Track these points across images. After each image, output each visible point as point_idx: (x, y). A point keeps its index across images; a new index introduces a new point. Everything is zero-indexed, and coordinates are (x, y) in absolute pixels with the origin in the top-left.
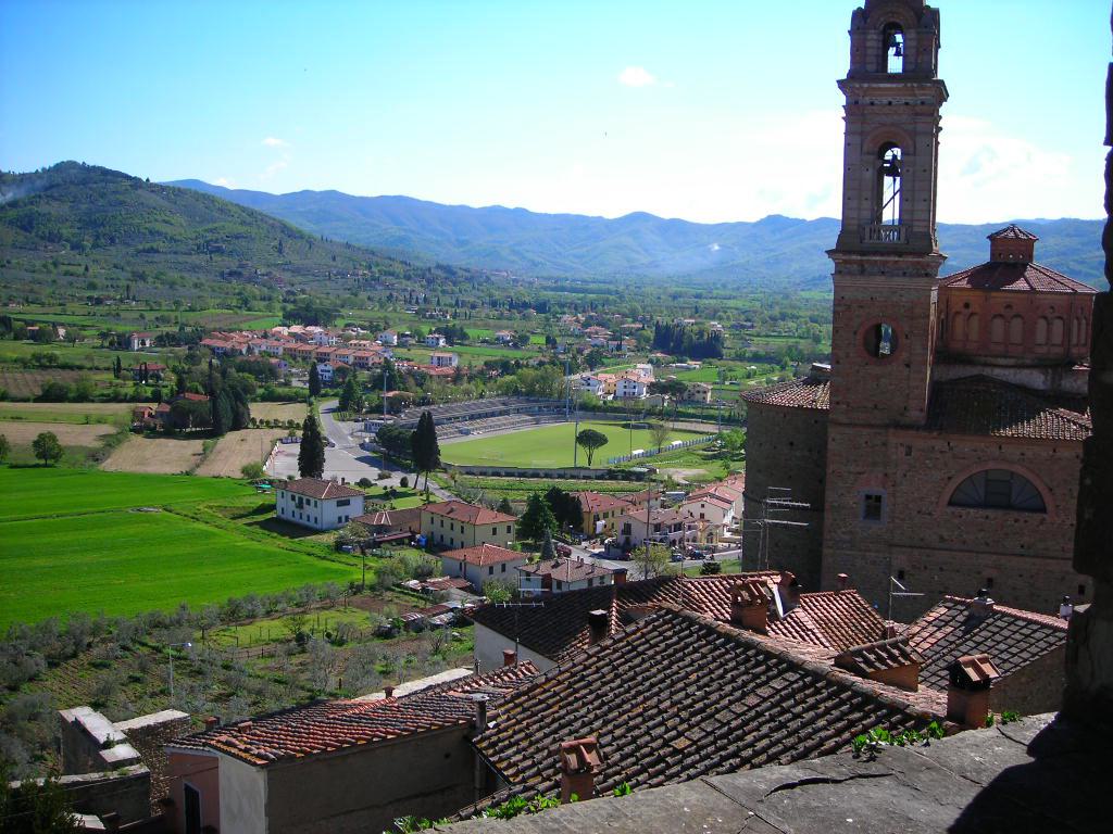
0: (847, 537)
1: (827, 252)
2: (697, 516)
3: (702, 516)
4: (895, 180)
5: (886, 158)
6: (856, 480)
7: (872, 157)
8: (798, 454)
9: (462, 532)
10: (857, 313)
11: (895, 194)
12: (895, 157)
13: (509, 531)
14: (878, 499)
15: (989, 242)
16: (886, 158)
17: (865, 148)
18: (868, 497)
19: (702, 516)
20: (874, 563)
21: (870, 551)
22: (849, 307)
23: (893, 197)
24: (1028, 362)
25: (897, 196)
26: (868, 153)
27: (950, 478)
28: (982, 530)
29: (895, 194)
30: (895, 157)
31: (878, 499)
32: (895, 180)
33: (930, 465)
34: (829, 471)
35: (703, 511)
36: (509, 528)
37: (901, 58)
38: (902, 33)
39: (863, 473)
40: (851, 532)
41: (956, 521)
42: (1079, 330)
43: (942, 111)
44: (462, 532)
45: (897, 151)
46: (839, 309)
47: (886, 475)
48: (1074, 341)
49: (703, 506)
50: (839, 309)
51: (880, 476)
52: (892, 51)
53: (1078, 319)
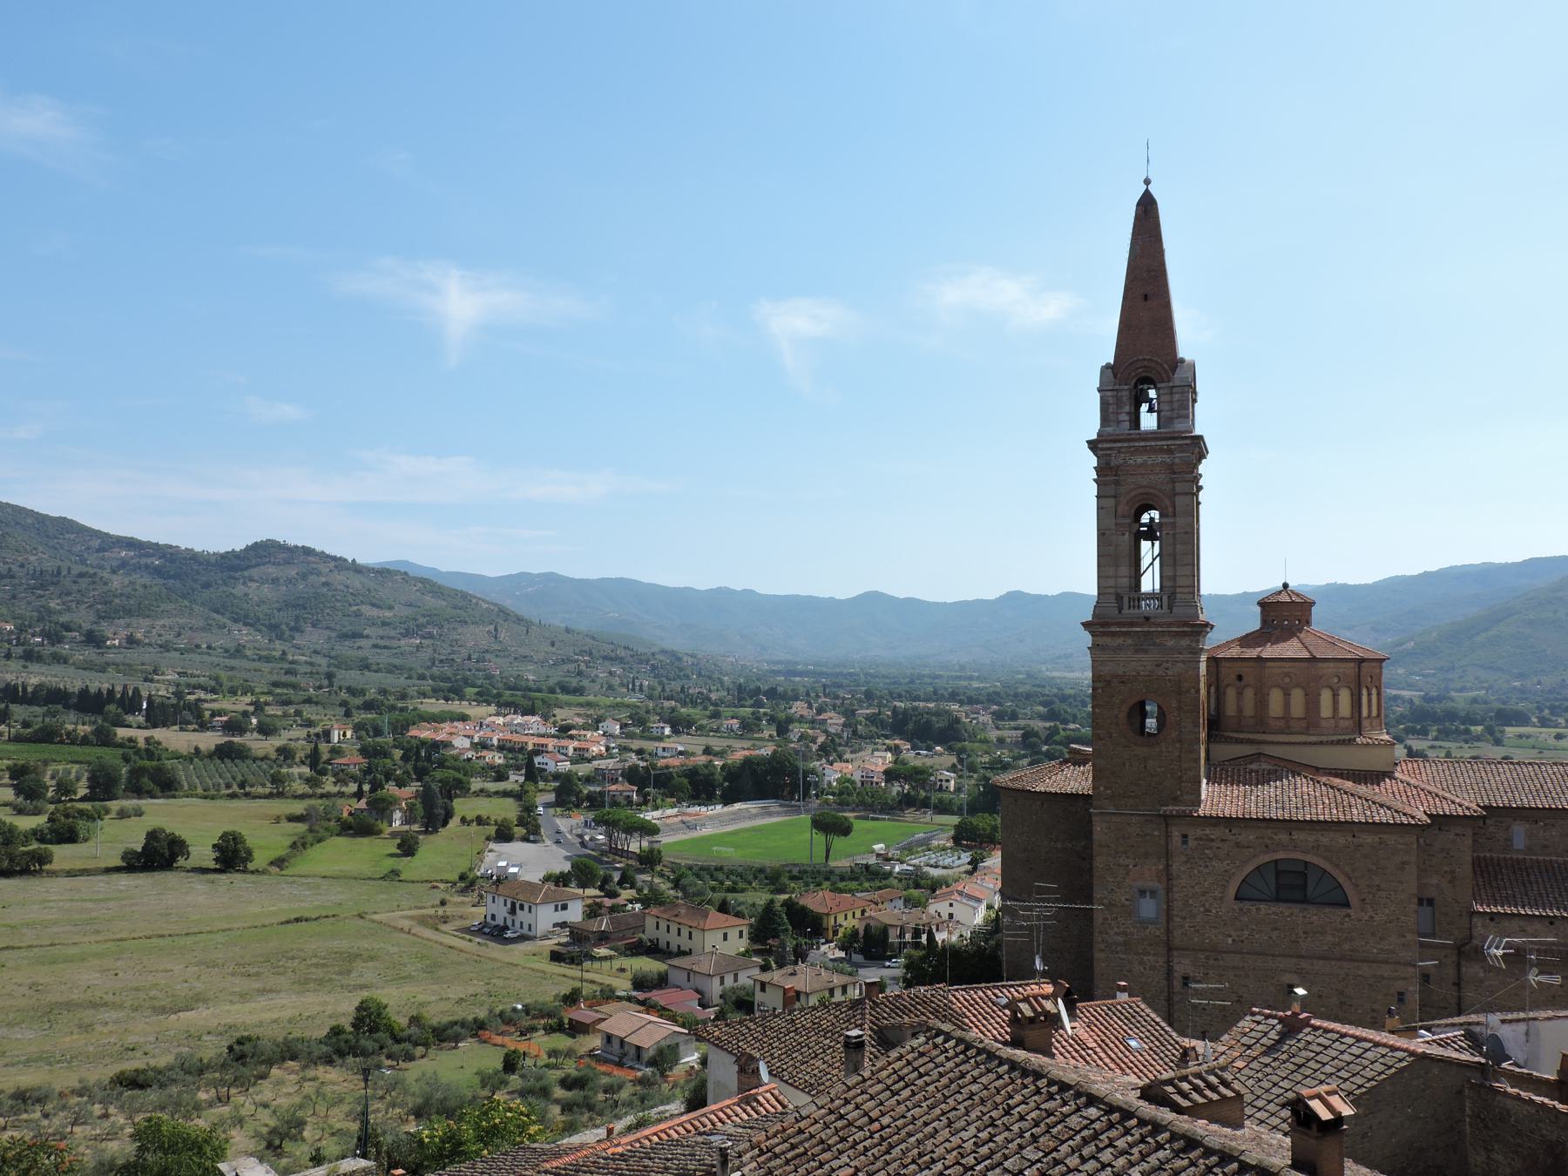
0: (1120, 939)
1: (1083, 624)
2: (945, 916)
3: (951, 916)
5: (1143, 521)
6: (1127, 874)
7: (1128, 521)
9: (690, 938)
11: (1154, 560)
12: (1152, 519)
13: (741, 936)
15: (1258, 609)
16: (1143, 521)
17: (1120, 511)
19: (951, 916)
20: (1152, 968)
21: (1149, 954)
23: (1152, 564)
25: (1157, 562)
26: (1124, 517)
28: (1276, 929)
29: (1154, 560)
30: (1152, 519)
33: (1211, 856)
35: (951, 910)
36: (741, 932)
38: (1155, 388)
40: (1125, 933)
43: (1202, 469)
44: (690, 938)
45: (1155, 514)
49: (951, 905)
50: (1098, 684)
52: (1144, 407)
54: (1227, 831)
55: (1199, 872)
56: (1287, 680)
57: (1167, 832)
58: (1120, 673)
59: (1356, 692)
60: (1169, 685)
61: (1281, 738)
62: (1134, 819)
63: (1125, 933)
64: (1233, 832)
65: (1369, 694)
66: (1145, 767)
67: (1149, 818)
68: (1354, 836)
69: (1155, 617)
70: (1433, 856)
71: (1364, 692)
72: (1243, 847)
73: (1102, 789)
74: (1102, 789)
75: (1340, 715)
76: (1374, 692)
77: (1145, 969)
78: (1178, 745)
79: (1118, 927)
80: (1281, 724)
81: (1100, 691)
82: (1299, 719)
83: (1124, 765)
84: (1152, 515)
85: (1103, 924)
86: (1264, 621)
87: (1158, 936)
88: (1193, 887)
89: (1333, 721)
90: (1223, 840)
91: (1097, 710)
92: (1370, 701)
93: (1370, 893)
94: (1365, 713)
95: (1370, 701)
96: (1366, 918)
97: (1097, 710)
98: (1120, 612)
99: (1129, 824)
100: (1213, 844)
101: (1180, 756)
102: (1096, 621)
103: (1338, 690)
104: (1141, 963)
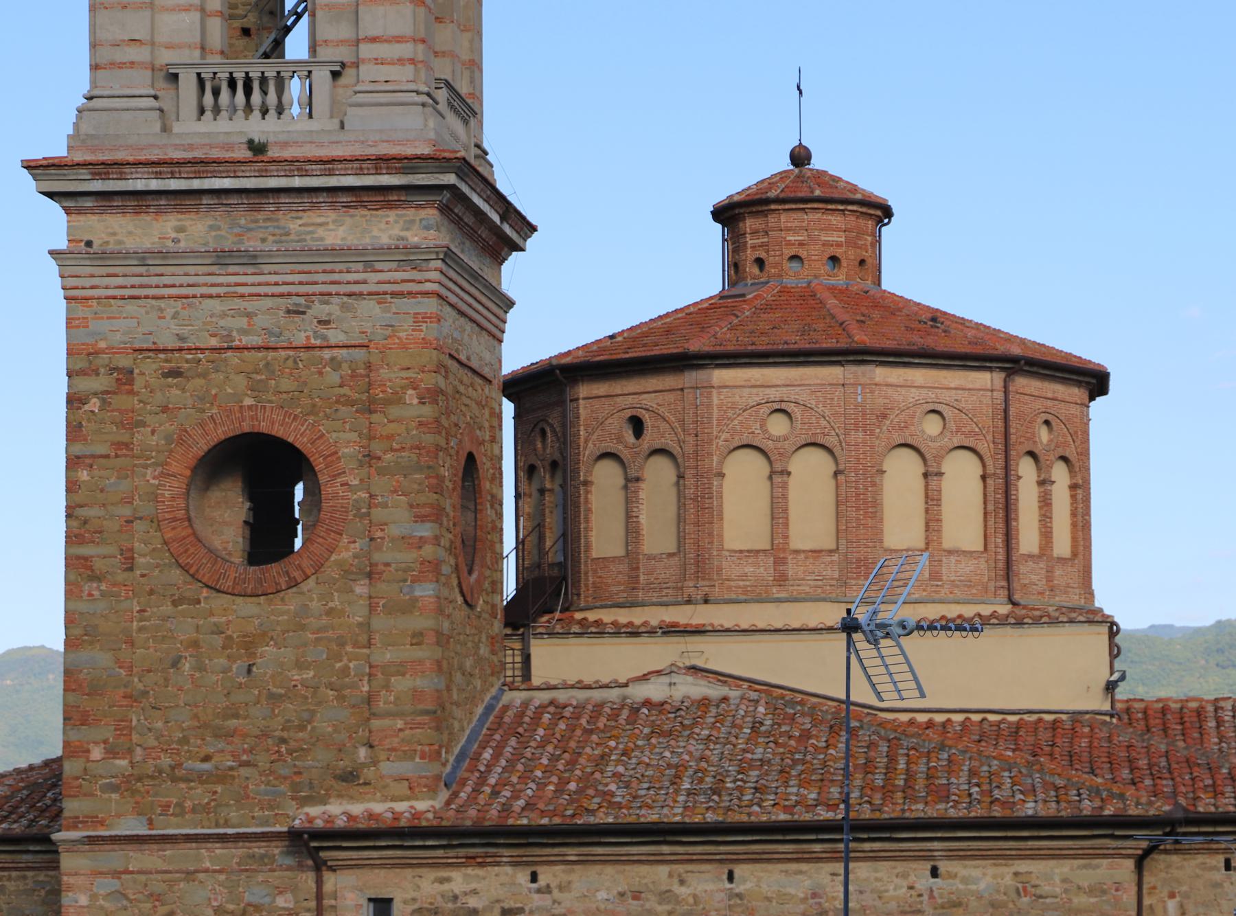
10: (159, 398)
22: (125, 378)
46: (87, 384)
50: (87, 384)
54: (523, 877)
56: (778, 426)
57: (319, 896)
58: (168, 341)
59: (995, 467)
60: (333, 377)
62: (208, 856)
64: (543, 881)
65: (1044, 482)
66: (249, 671)
67: (258, 849)
68: (935, 873)
69: (285, 145)
71: (1026, 470)
73: (97, 753)
74: (97, 753)
75: (947, 544)
76: (1060, 474)
78: (361, 589)
81: (94, 404)
82: (817, 553)
83: (175, 664)
86: (734, 269)
91: (84, 475)
92: (1045, 502)
94: (1028, 539)
95: (1045, 502)
97: (84, 475)
98: (165, 129)
99: (190, 875)
101: (366, 626)
102: (79, 157)
103: (939, 458)
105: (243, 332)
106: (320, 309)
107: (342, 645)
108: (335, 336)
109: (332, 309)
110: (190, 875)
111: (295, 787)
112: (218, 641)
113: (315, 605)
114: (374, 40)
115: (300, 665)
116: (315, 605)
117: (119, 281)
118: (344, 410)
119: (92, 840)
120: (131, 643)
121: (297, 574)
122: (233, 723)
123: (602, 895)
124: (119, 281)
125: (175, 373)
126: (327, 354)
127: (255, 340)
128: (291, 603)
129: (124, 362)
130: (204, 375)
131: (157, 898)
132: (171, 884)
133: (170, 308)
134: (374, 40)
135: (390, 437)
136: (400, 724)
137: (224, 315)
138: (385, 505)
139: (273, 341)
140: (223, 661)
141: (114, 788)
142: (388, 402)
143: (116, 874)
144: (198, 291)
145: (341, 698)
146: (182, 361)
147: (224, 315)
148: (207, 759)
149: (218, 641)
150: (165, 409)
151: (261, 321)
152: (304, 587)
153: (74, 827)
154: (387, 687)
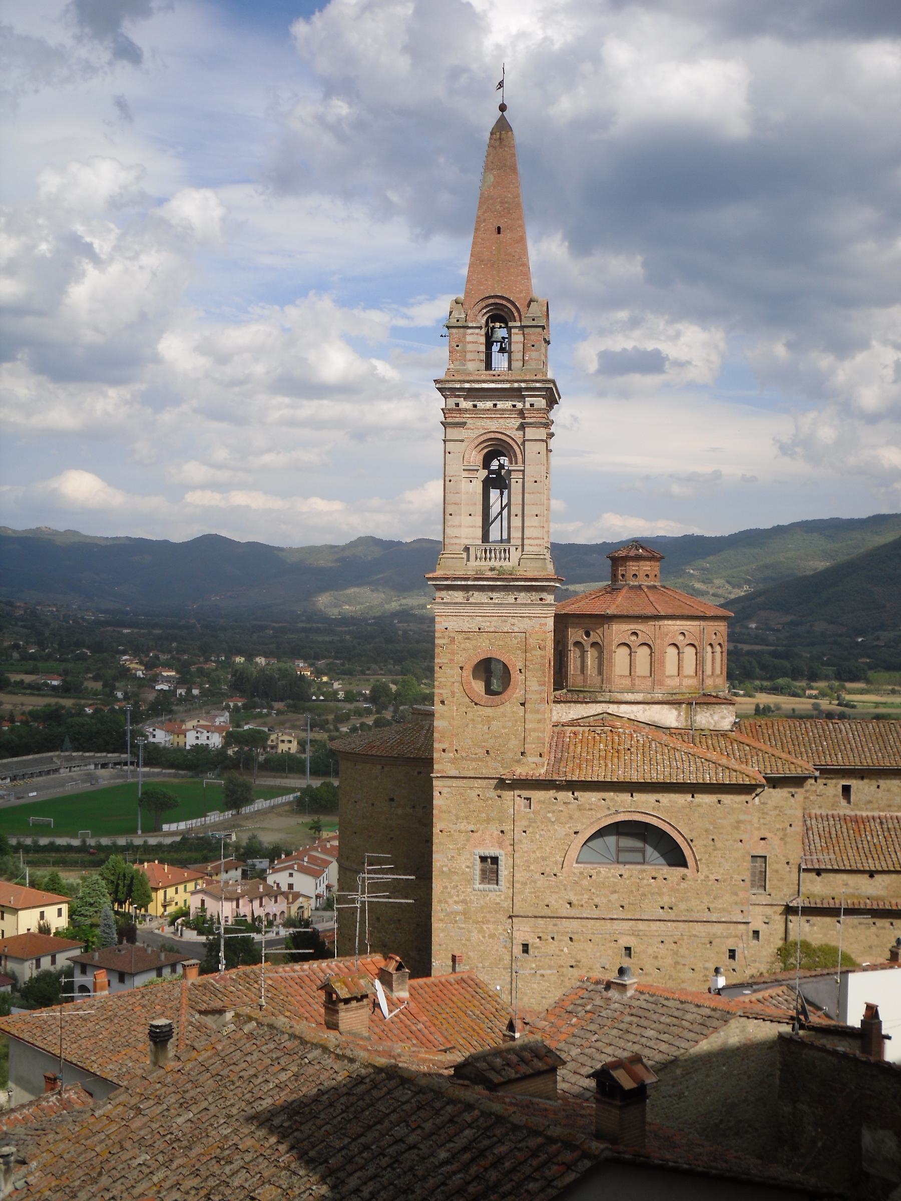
0: (459, 908)
2: (284, 888)
3: (291, 886)
4: (502, 494)
6: (468, 840)
8: (400, 811)
10: (463, 646)
11: (502, 509)
14: (495, 860)
18: (483, 859)
20: (492, 936)
21: (488, 922)
22: (453, 640)
23: (501, 513)
24: (659, 697)
27: (576, 833)
28: (615, 892)
29: (502, 509)
31: (495, 860)
32: (502, 494)
33: (553, 819)
34: (436, 830)
35: (291, 880)
37: (506, 355)
39: (477, 832)
40: (464, 902)
41: (585, 882)
42: (713, 659)
47: (502, 832)
48: (709, 671)
51: (497, 833)
53: (711, 645)
55: (541, 835)
60: (516, 642)
61: (629, 697)
63: (464, 902)
70: (767, 814)
72: (585, 809)
77: (484, 937)
79: (458, 896)
80: (627, 682)
83: (467, 726)
84: (502, 462)
85: (442, 892)
87: (499, 903)
88: (534, 852)
89: (677, 680)
90: (564, 803)
93: (706, 853)
96: (702, 877)
99: (471, 788)
100: (556, 807)
104: (481, 931)
105: (488, 627)
106: (511, 620)
107: (516, 722)
108: (516, 630)
109: (515, 621)
110: (471, 788)
111: (502, 764)
112: (480, 719)
113: (508, 709)
114: (529, 538)
115: (504, 728)
116: (508, 709)
117: (452, 611)
118: (519, 652)
119: (441, 777)
120: (453, 719)
121: (503, 701)
122: (484, 744)
123: (593, 799)
124: (452, 611)
125: (468, 638)
126: (513, 634)
127: (492, 630)
128: (501, 709)
129: (452, 635)
130: (476, 639)
131: (461, 794)
132: (466, 790)
133: (467, 619)
134: (529, 538)
135: (532, 660)
136: (534, 746)
137: (482, 622)
138: (530, 681)
139: (497, 630)
140: (481, 726)
141: (449, 762)
142: (532, 649)
143: (449, 787)
144: (475, 614)
145: (516, 738)
146: (470, 635)
147: (482, 622)
148: (476, 754)
149: (480, 719)
150: (464, 650)
151: (493, 624)
152: (506, 704)
153: (437, 773)
154: (530, 735)
